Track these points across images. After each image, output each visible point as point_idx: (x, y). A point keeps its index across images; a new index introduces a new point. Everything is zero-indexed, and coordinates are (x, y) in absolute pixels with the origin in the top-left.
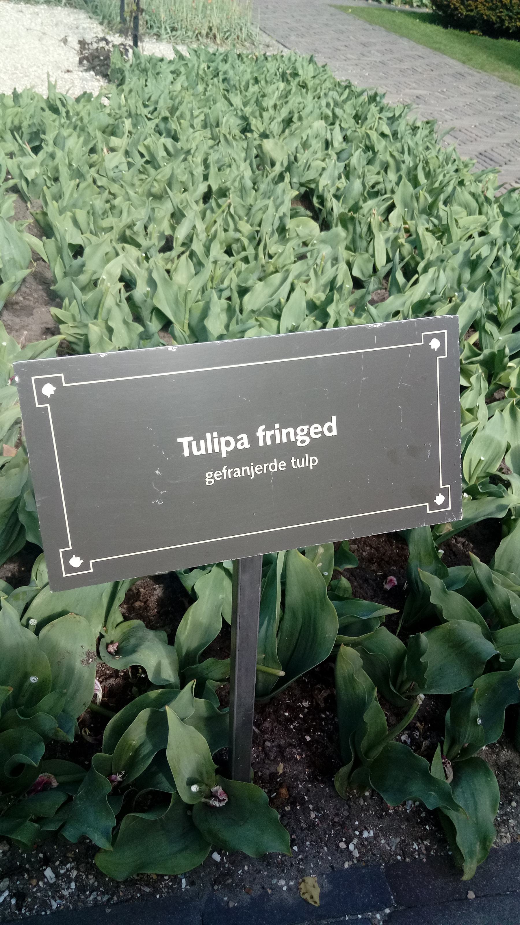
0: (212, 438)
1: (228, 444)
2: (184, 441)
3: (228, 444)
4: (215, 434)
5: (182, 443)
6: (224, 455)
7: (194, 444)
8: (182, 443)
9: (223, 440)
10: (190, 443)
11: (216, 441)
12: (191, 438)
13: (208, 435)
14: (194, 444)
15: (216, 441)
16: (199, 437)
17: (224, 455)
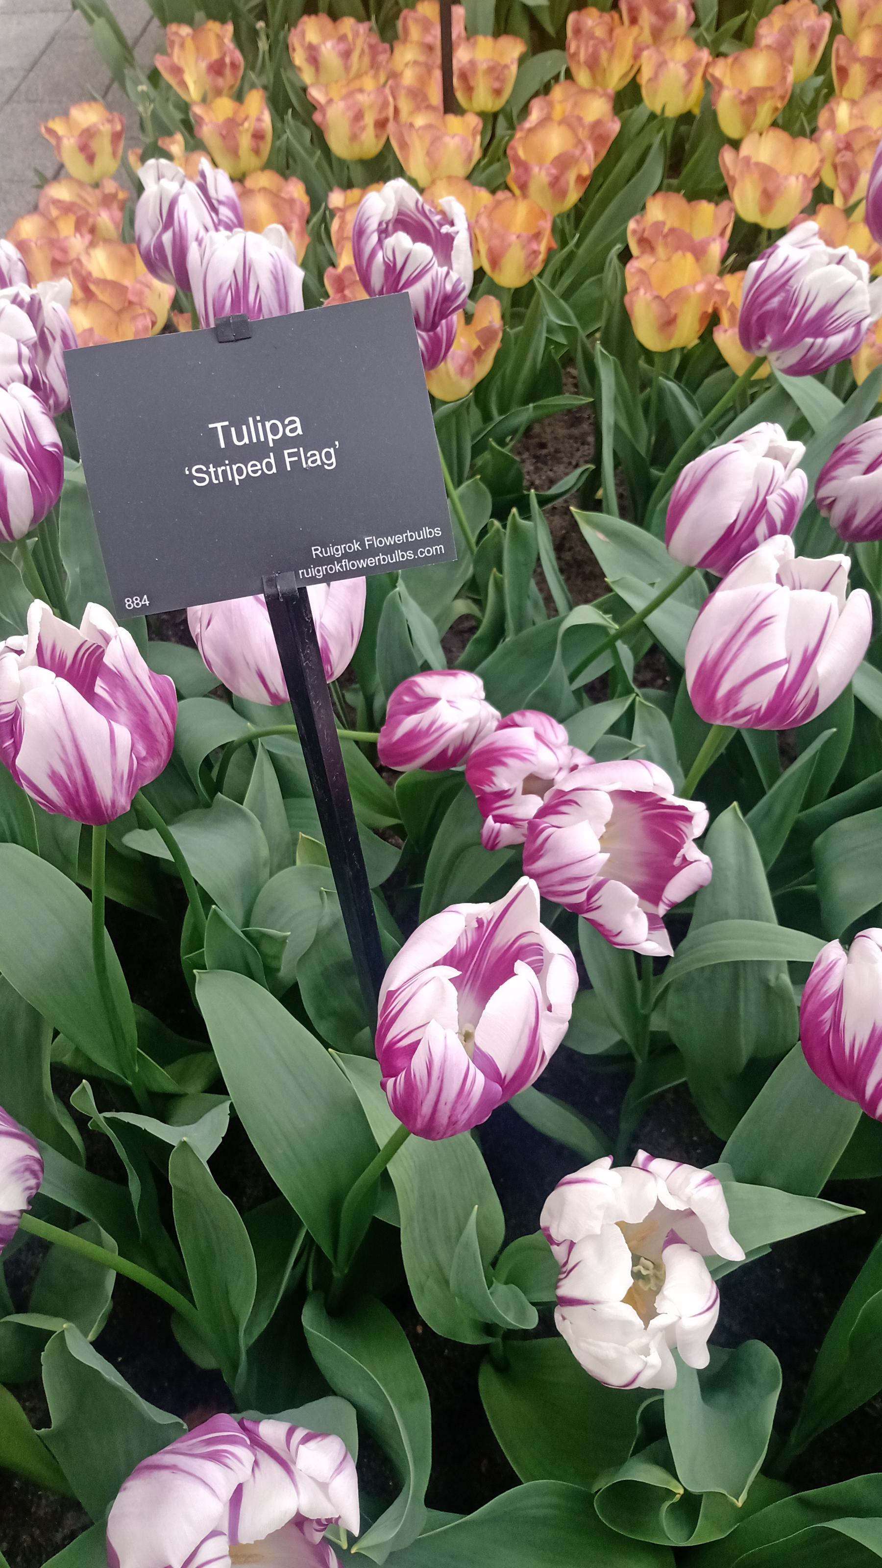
1: (274, 429)
2: (219, 425)
3: (274, 429)
4: (258, 418)
6: (271, 445)
7: (233, 429)
9: (268, 425)
10: (226, 430)
11: (260, 425)
12: (227, 423)
13: (251, 419)
14: (233, 429)
15: (260, 425)
16: (238, 422)
17: (271, 445)
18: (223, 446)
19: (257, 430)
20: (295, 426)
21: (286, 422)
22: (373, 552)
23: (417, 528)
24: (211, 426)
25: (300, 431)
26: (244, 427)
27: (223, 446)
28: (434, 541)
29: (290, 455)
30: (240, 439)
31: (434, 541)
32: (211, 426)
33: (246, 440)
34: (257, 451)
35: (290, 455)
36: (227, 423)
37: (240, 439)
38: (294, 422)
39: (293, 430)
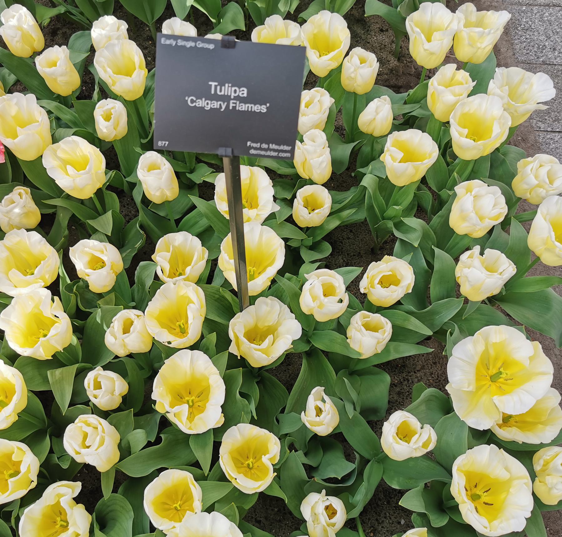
0: (229, 86)
2: (213, 84)
4: (230, 85)
5: (211, 85)
6: (232, 97)
7: (218, 88)
8: (211, 85)
9: (233, 89)
10: (216, 86)
11: (230, 88)
12: (216, 84)
13: (227, 85)
14: (218, 88)
15: (230, 88)
16: (222, 84)
17: (232, 97)
18: (213, 92)
19: (228, 90)
20: (244, 92)
21: (241, 89)
22: (260, 149)
23: (280, 145)
24: (210, 83)
25: (245, 95)
26: (223, 88)
27: (213, 92)
28: (285, 151)
29: (233, 103)
30: (221, 91)
31: (285, 151)
32: (210, 83)
33: (222, 93)
34: (226, 98)
35: (233, 103)
36: (216, 84)
37: (221, 91)
38: (243, 90)
39: (243, 94)
